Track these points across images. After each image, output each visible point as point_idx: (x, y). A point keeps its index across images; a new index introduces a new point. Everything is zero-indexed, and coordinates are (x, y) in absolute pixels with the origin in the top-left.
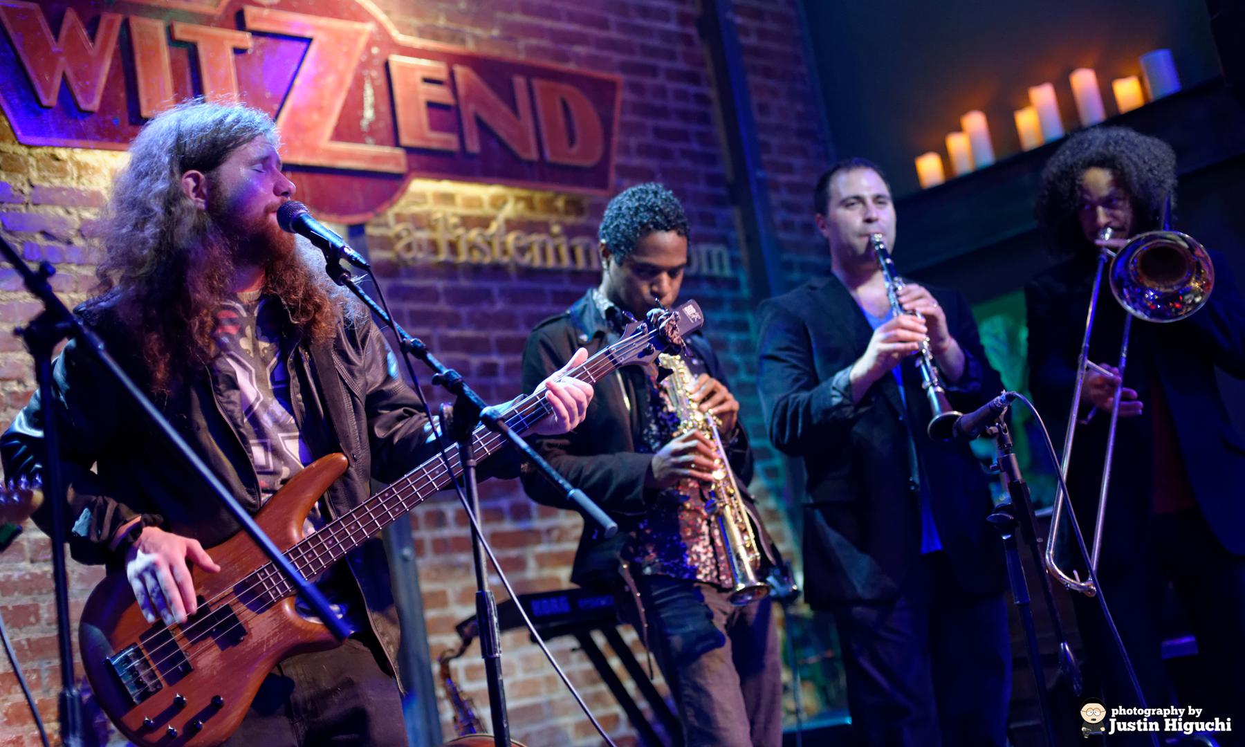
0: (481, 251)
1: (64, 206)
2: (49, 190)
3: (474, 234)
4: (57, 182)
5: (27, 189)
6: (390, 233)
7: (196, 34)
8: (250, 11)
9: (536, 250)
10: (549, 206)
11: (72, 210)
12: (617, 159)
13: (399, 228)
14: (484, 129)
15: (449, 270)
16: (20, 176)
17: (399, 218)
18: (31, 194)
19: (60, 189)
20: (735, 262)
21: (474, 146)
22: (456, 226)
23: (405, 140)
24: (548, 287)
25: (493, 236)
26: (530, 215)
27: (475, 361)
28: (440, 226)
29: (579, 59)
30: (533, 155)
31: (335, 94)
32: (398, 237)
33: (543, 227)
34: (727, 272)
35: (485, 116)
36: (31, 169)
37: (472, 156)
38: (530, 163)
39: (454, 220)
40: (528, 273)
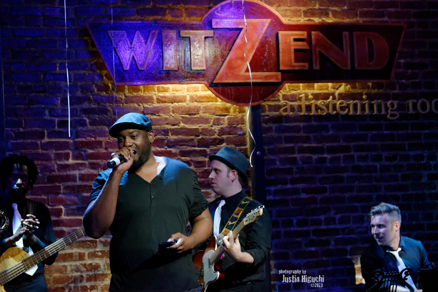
0: (322, 109)
1: (136, 103)
2: (132, 97)
3: (319, 102)
4: (135, 94)
5: (123, 97)
7: (189, 34)
8: (214, 21)
11: (140, 104)
13: (282, 102)
14: (323, 58)
15: (307, 118)
16: (121, 93)
17: (285, 97)
18: (125, 99)
19: (136, 97)
21: (317, 67)
23: (282, 68)
25: (329, 102)
26: (352, 91)
27: (315, 157)
28: (303, 99)
29: (390, 15)
31: (249, 52)
35: (325, 53)
36: (125, 89)
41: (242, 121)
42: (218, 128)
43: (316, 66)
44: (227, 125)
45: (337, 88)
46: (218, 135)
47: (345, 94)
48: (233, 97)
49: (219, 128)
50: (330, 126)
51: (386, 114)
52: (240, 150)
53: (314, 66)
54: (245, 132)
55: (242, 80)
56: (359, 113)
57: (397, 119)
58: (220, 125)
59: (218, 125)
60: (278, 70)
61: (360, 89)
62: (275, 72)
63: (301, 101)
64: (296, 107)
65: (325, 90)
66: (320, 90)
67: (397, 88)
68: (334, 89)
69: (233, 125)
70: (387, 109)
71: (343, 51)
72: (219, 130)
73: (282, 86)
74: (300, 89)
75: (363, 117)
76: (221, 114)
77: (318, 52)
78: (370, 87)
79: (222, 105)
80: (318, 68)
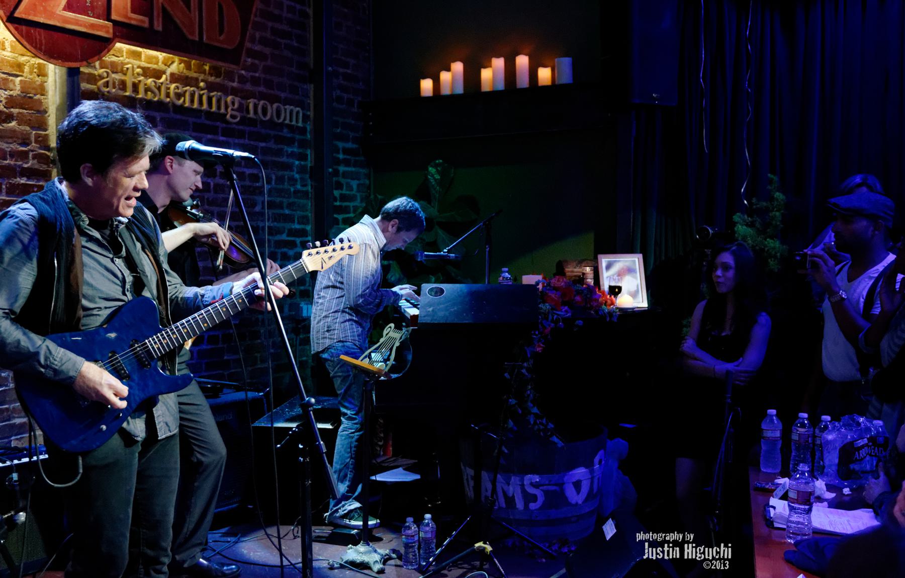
0: (152, 92)
3: (150, 81)
6: (96, 73)
9: (187, 95)
10: (201, 71)
12: (248, 45)
14: (167, 17)
20: (306, 118)
21: (158, 26)
22: (138, 74)
23: (114, 17)
24: (191, 120)
25: (162, 83)
28: (130, 71)
30: (197, 39)
32: (101, 77)
33: (193, 82)
34: (300, 124)
35: (169, 9)
37: (158, 32)
38: (193, 41)
39: (139, 70)
40: (180, 109)
41: (42, 91)
42: (4, 94)
43: (158, 26)
44: (19, 93)
45: (168, 64)
46: (5, 107)
47: (178, 75)
48: (43, 47)
49: (6, 95)
50: (158, 119)
51: (226, 113)
52: (38, 136)
53: (155, 23)
54: (47, 109)
55: (59, 22)
56: (196, 106)
57: (235, 123)
58: (8, 91)
59: (5, 90)
60: (108, 19)
61: (195, 72)
62: (104, 20)
63: (125, 74)
64: (117, 82)
65: (155, 64)
66: (149, 63)
67: (236, 80)
68: (165, 65)
69: (28, 94)
70: (227, 107)
71: (190, 11)
72: (6, 98)
73: (112, 44)
74: (123, 56)
75: (197, 113)
76: (10, 72)
77: (160, 5)
78: (207, 72)
79: (13, 58)
80: (160, 29)
